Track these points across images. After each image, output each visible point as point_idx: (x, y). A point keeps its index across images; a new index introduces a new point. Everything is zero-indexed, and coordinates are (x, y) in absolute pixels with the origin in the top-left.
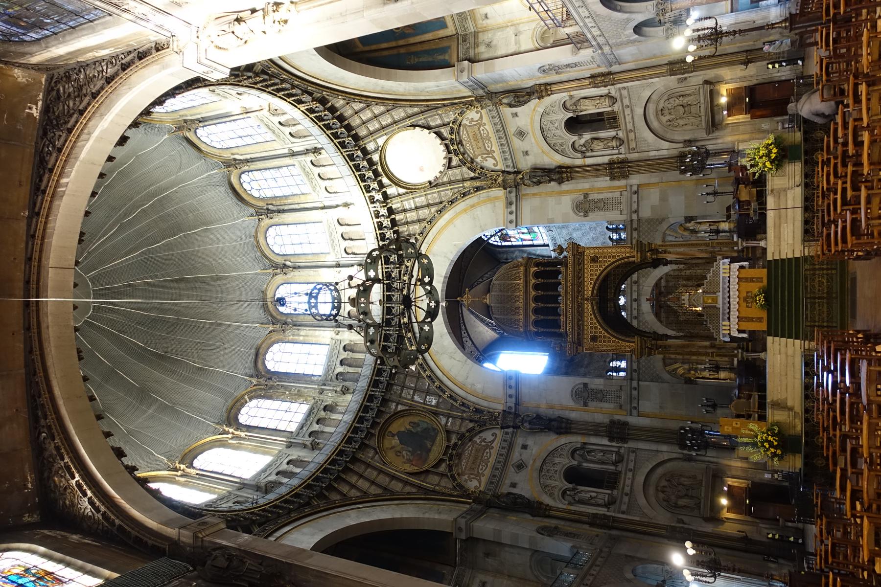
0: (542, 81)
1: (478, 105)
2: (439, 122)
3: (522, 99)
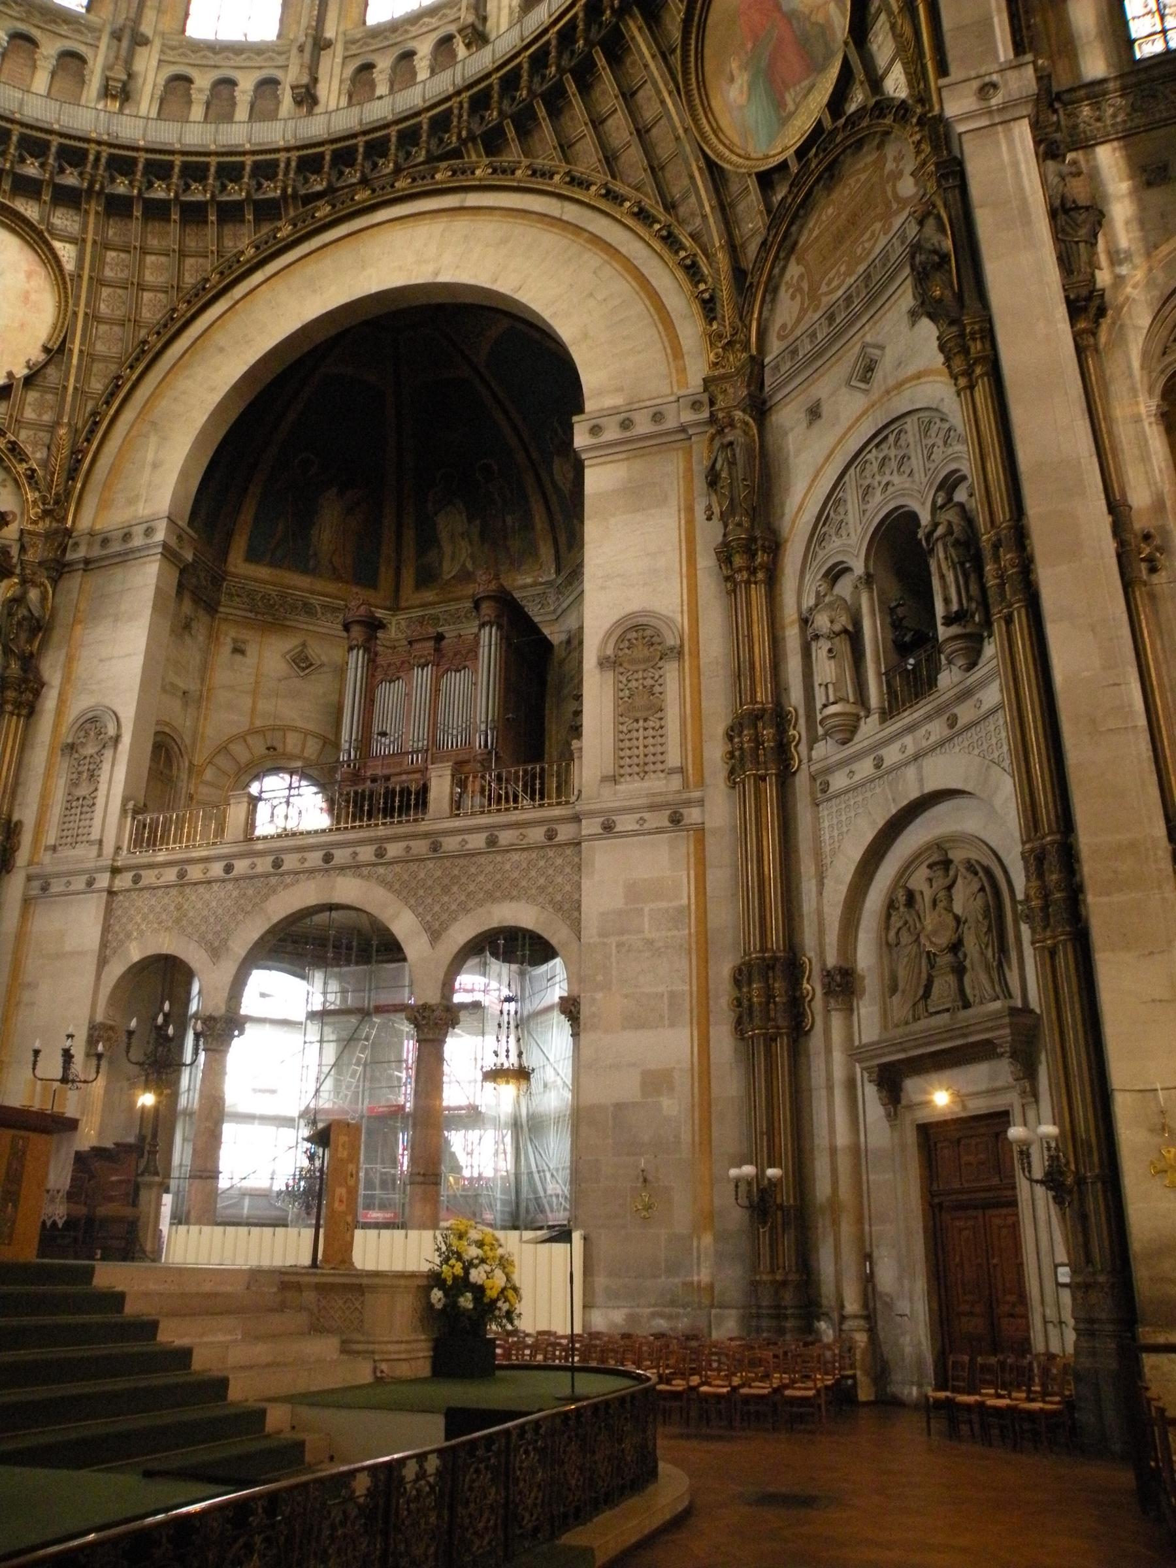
0: (49, 702)
1: (41, 527)
2: (29, 414)
3: (23, 636)
